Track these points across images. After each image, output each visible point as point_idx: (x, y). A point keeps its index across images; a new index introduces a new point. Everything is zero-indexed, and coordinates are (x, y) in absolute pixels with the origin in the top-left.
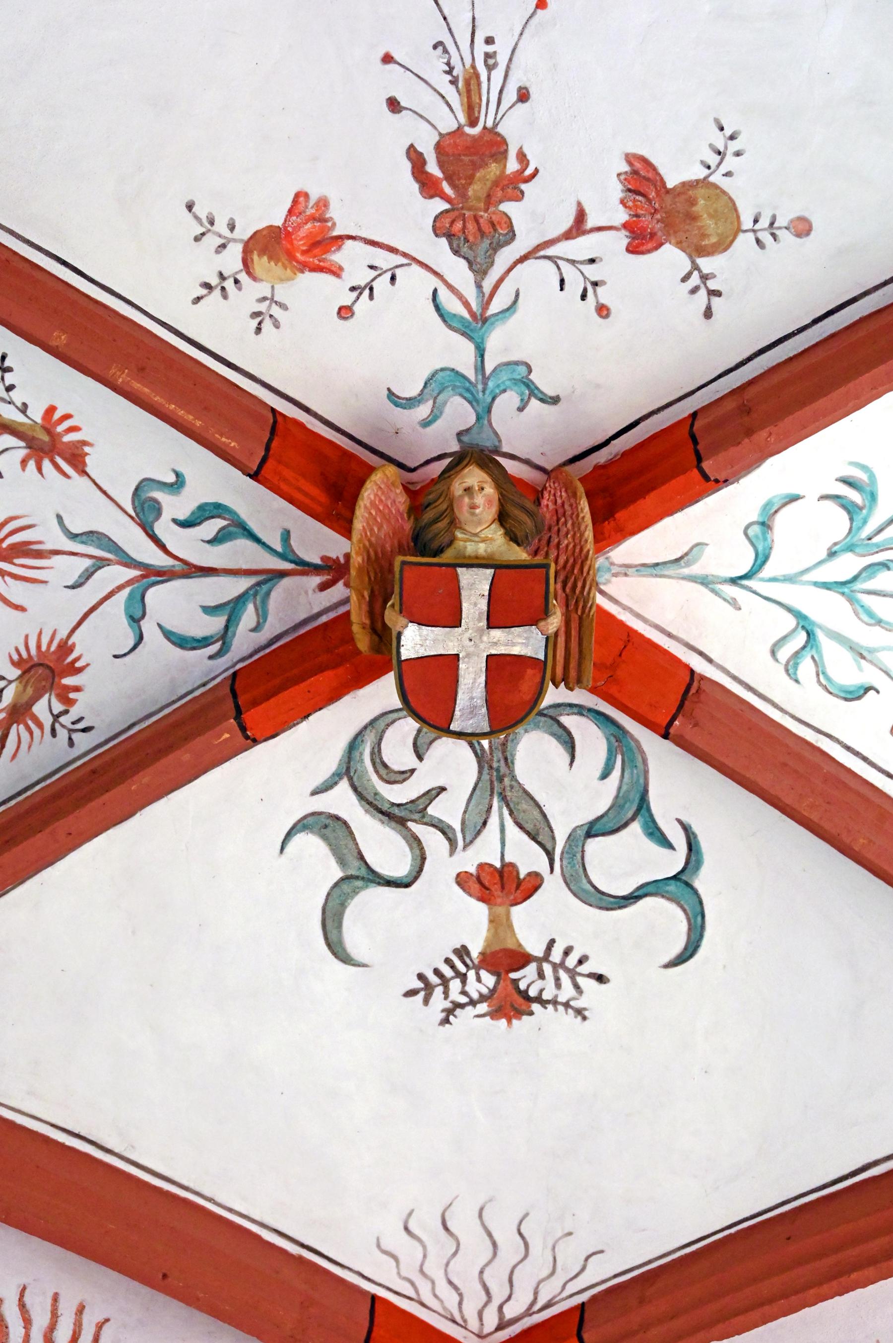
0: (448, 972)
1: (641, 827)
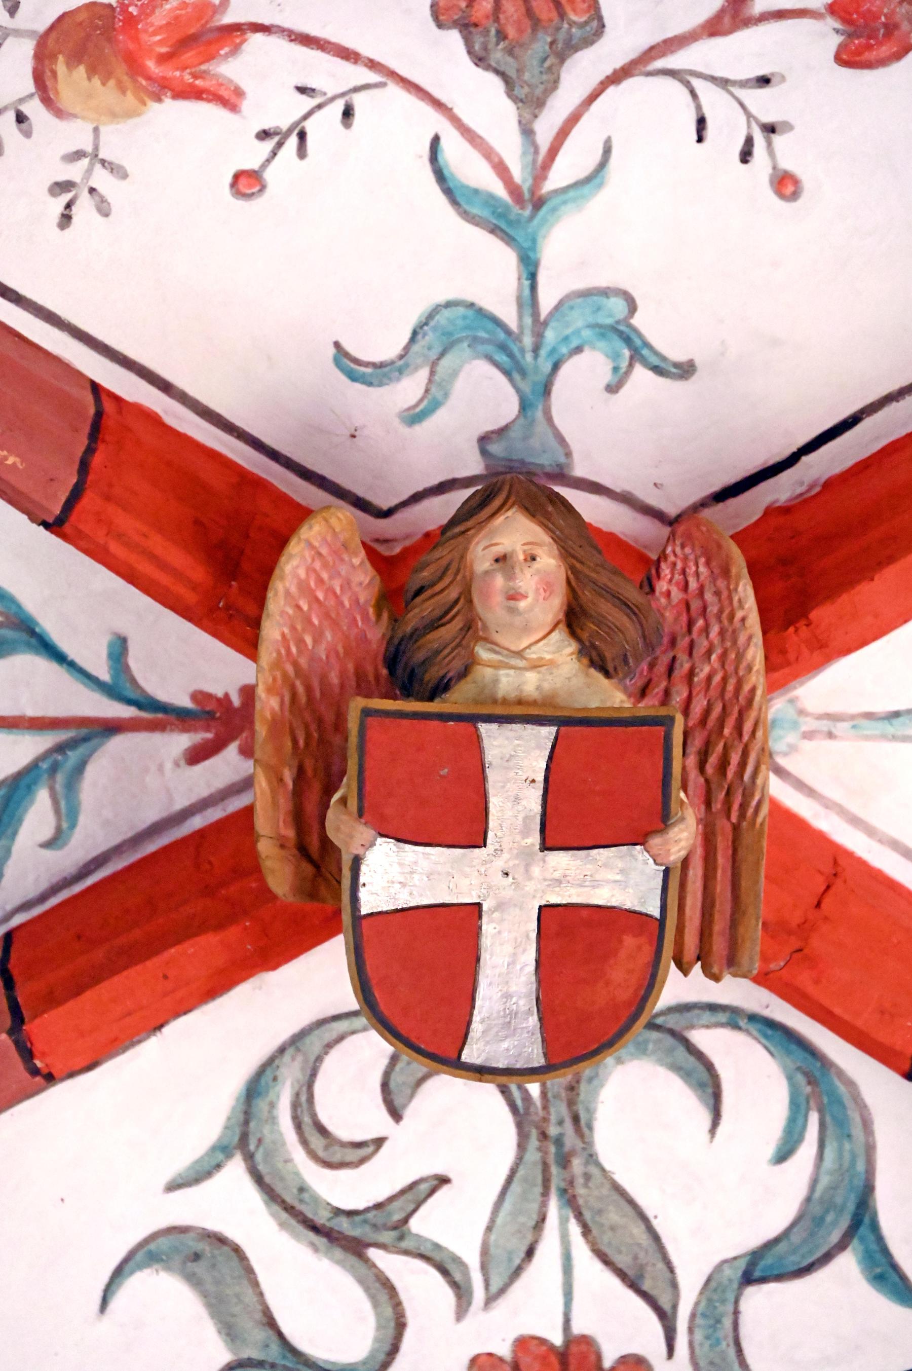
1: (859, 1262)
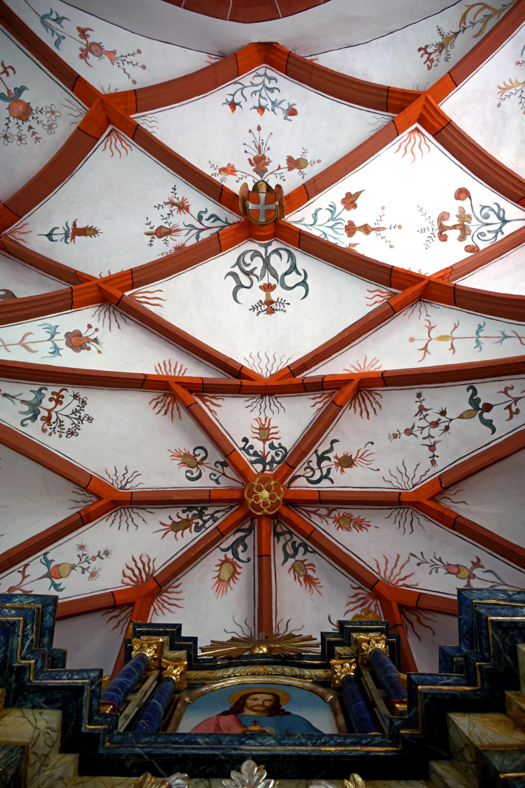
0: (258, 305)
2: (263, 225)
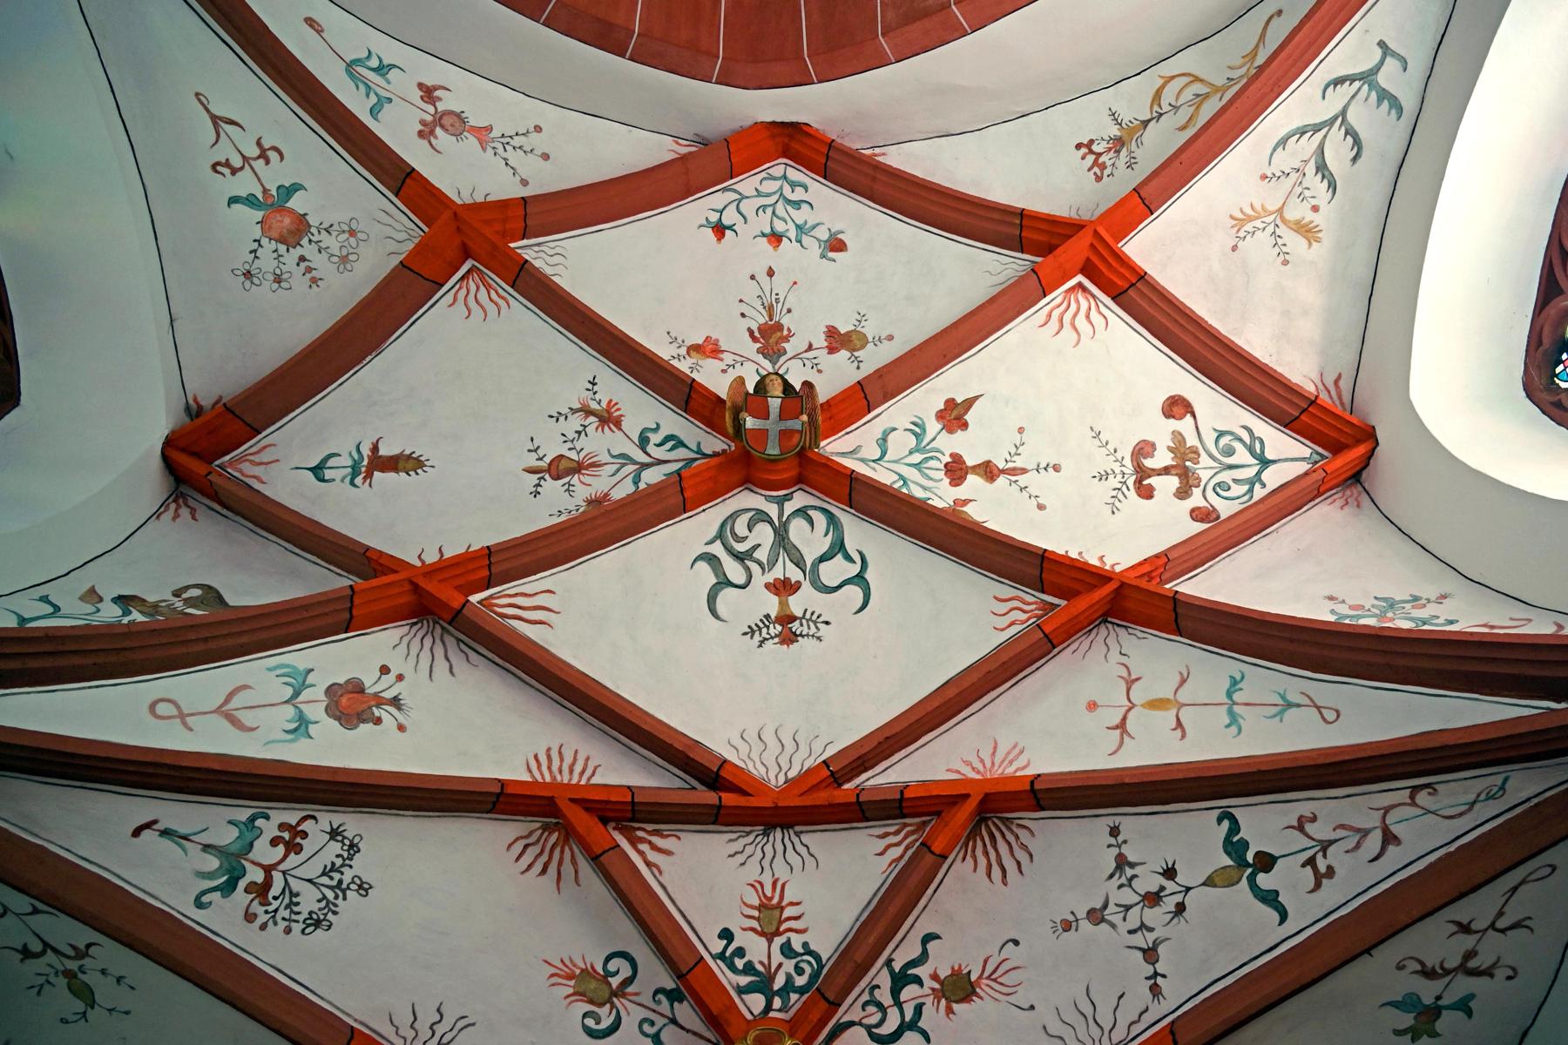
0: (761, 625)
2: (773, 461)
